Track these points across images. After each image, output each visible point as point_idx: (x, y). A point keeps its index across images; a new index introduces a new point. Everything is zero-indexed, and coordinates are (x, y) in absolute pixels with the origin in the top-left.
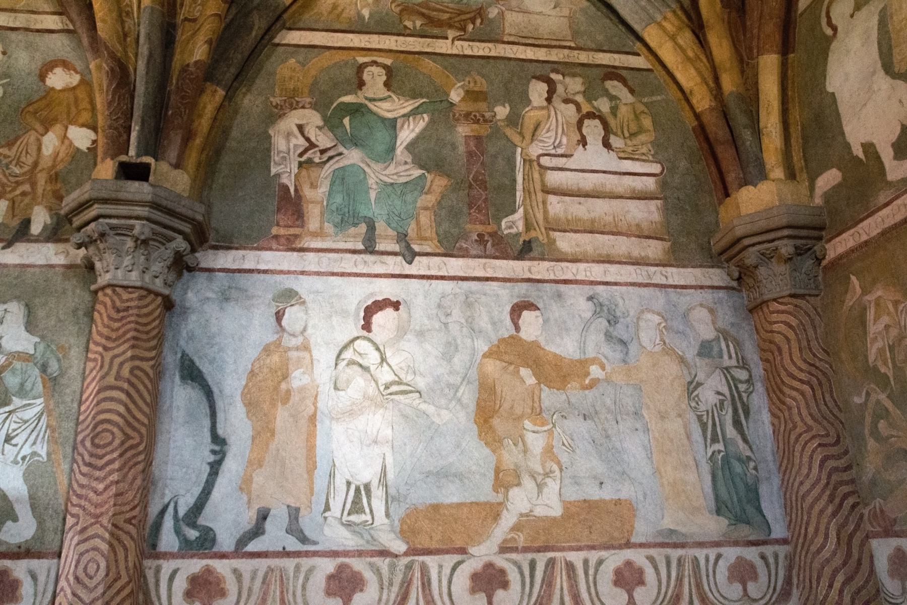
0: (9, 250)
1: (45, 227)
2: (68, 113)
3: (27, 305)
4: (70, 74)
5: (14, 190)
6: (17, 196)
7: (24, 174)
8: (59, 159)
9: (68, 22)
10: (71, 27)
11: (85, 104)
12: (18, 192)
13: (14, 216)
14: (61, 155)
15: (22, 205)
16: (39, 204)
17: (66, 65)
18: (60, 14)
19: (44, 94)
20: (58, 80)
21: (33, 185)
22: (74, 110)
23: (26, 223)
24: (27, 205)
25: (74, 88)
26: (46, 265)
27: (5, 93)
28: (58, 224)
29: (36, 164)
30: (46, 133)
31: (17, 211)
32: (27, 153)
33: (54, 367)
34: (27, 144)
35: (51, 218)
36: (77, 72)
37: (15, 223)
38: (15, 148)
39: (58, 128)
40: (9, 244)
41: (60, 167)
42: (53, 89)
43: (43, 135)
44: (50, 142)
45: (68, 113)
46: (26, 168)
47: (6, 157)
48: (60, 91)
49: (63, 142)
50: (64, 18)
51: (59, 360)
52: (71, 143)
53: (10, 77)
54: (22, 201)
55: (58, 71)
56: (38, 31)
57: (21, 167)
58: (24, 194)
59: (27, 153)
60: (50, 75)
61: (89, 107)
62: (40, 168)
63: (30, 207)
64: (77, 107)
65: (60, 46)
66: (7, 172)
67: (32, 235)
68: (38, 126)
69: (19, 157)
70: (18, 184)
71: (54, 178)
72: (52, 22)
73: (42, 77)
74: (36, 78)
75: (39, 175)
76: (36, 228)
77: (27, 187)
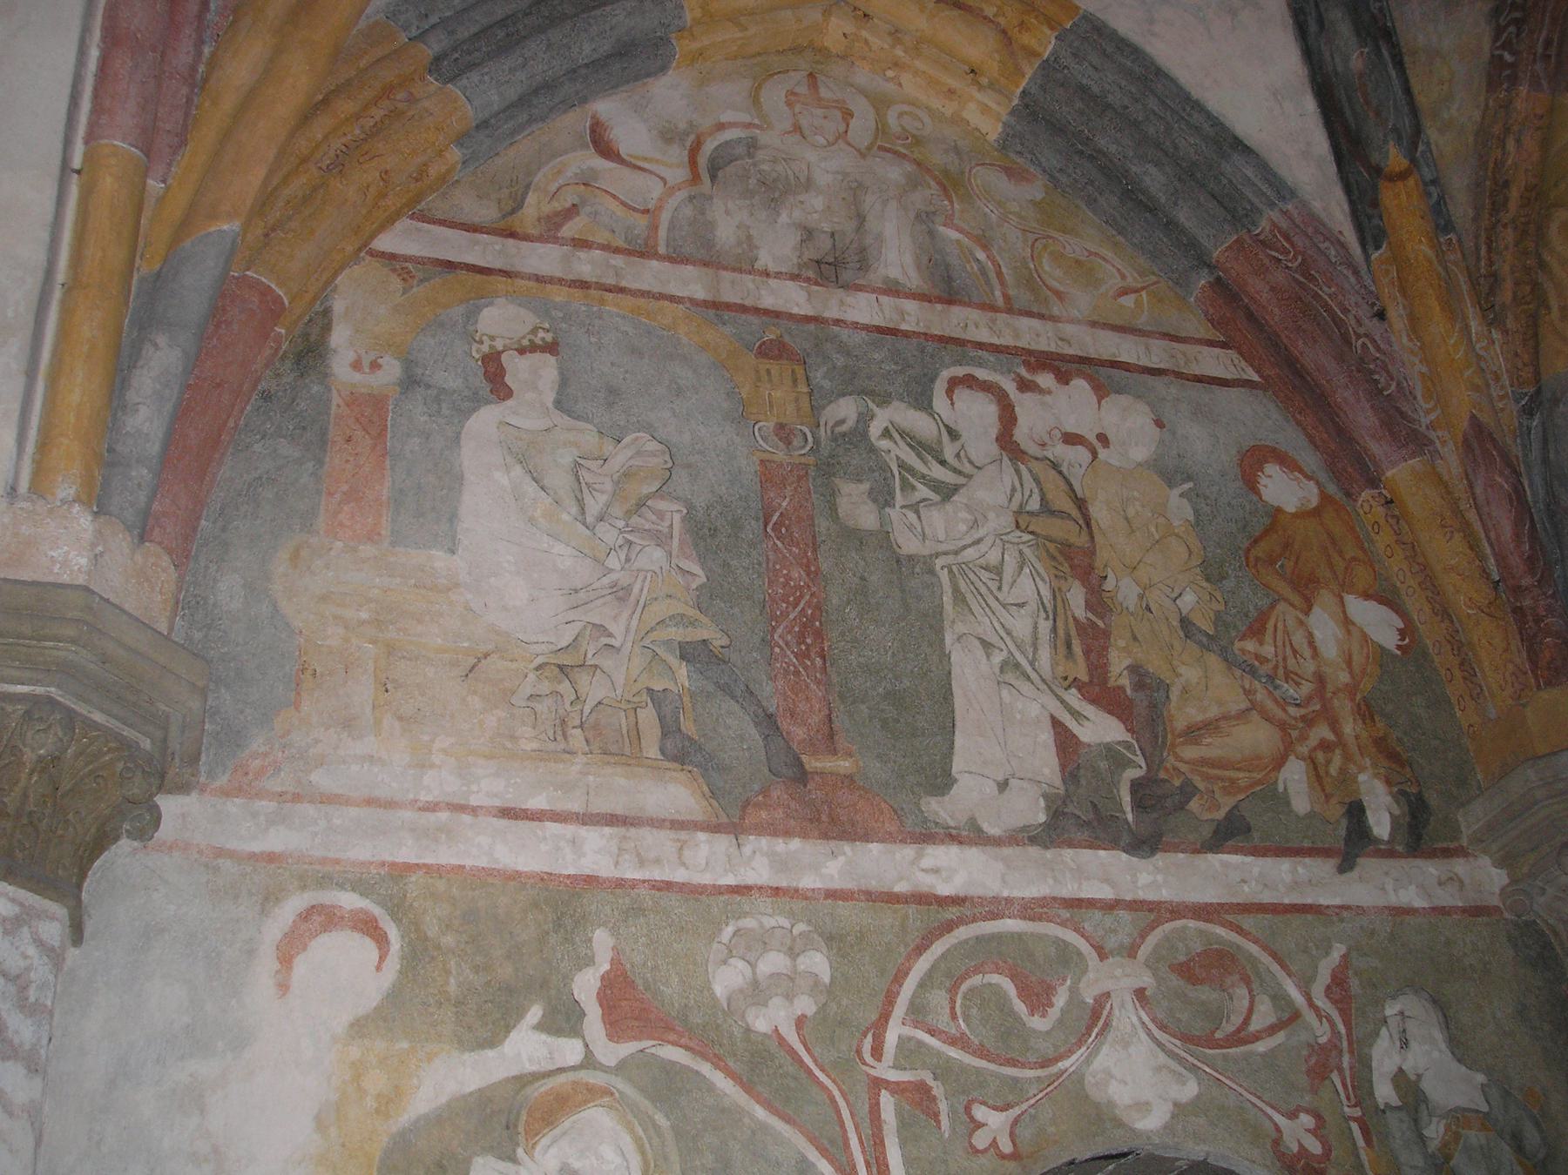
0: (1354, 874)
1: (1395, 820)
2: (1331, 566)
3: (1435, 1002)
4: (1297, 479)
5: (1303, 738)
6: (1315, 749)
7: (1309, 699)
8: (1357, 669)
9: (1243, 364)
10: (1256, 378)
11: (1351, 551)
12: (1313, 741)
13: (1328, 797)
14: (1358, 659)
15: (1333, 770)
16: (1362, 769)
17: (1283, 460)
18: (1224, 345)
19: (1267, 521)
20: (1284, 490)
21: (1334, 725)
22: (1340, 565)
23: (1356, 812)
24: (1342, 771)
25: (1316, 512)
26: (1434, 909)
27: (1196, 512)
28: (1413, 816)
29: (1320, 679)
30: (1310, 608)
31: (1328, 789)
32: (1295, 652)
33: (1532, 1137)
34: (1286, 632)
35: (1398, 802)
36: (1309, 478)
37: (1336, 811)
38: (1268, 637)
39: (1325, 597)
40: (1346, 866)
41: (1367, 685)
42: (1279, 510)
43: (1307, 612)
44: (1323, 626)
45: (1331, 566)
46: (1307, 688)
47: (1263, 660)
48: (1295, 516)
49: (1349, 632)
50: (1232, 353)
51: (1537, 1124)
52: (1365, 637)
53: (1189, 478)
54: (1328, 762)
55: (1272, 469)
56: (1199, 379)
57: (1298, 684)
58: (1325, 746)
59: (1295, 652)
60: (1263, 480)
61: (1360, 554)
62: (1330, 688)
63: (1346, 779)
64: (1341, 553)
65: (1258, 417)
66: (1277, 693)
67: (1377, 841)
68: (1286, 590)
69: (1285, 659)
70: (1309, 722)
71: (1366, 712)
72: (1215, 362)
73: (1251, 485)
74: (1240, 483)
75: (1336, 702)
76: (1381, 825)
77: (1323, 732)
